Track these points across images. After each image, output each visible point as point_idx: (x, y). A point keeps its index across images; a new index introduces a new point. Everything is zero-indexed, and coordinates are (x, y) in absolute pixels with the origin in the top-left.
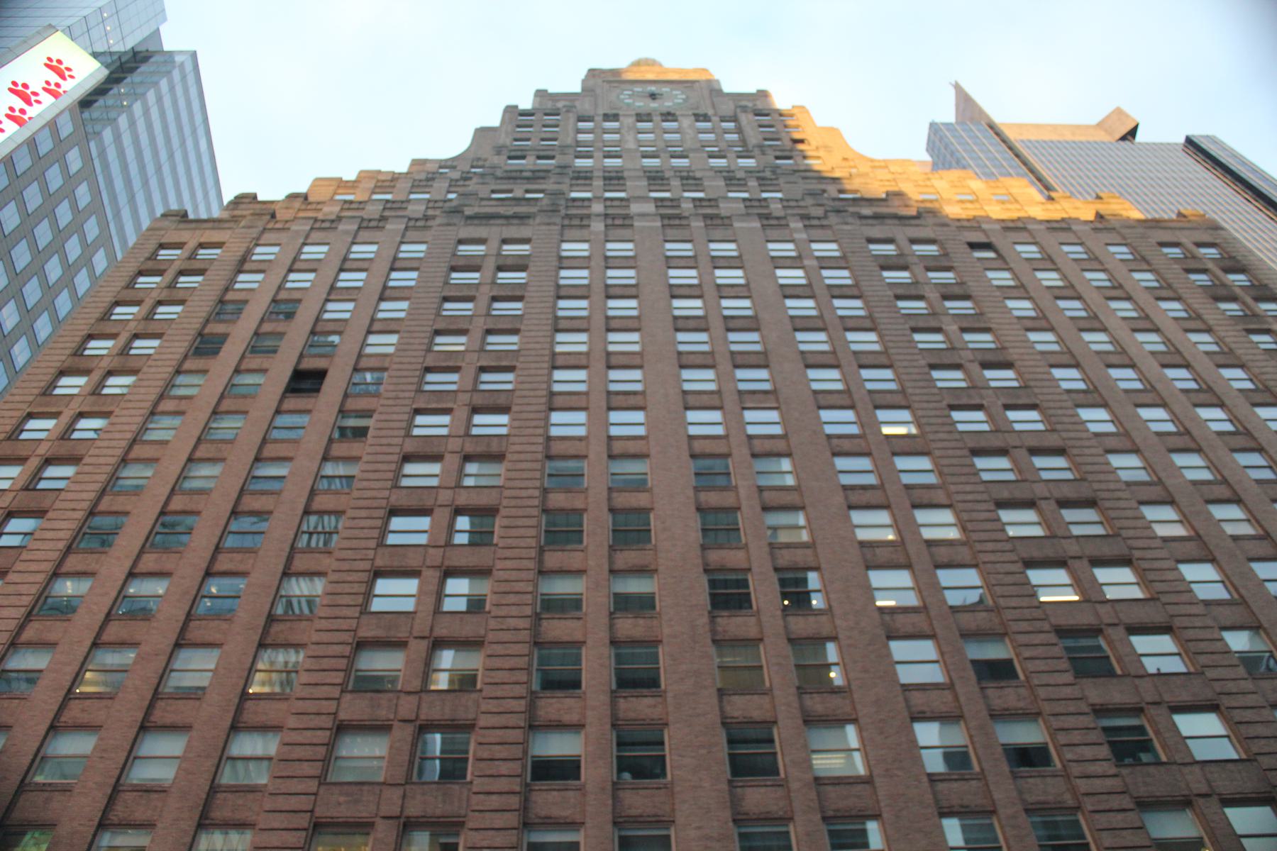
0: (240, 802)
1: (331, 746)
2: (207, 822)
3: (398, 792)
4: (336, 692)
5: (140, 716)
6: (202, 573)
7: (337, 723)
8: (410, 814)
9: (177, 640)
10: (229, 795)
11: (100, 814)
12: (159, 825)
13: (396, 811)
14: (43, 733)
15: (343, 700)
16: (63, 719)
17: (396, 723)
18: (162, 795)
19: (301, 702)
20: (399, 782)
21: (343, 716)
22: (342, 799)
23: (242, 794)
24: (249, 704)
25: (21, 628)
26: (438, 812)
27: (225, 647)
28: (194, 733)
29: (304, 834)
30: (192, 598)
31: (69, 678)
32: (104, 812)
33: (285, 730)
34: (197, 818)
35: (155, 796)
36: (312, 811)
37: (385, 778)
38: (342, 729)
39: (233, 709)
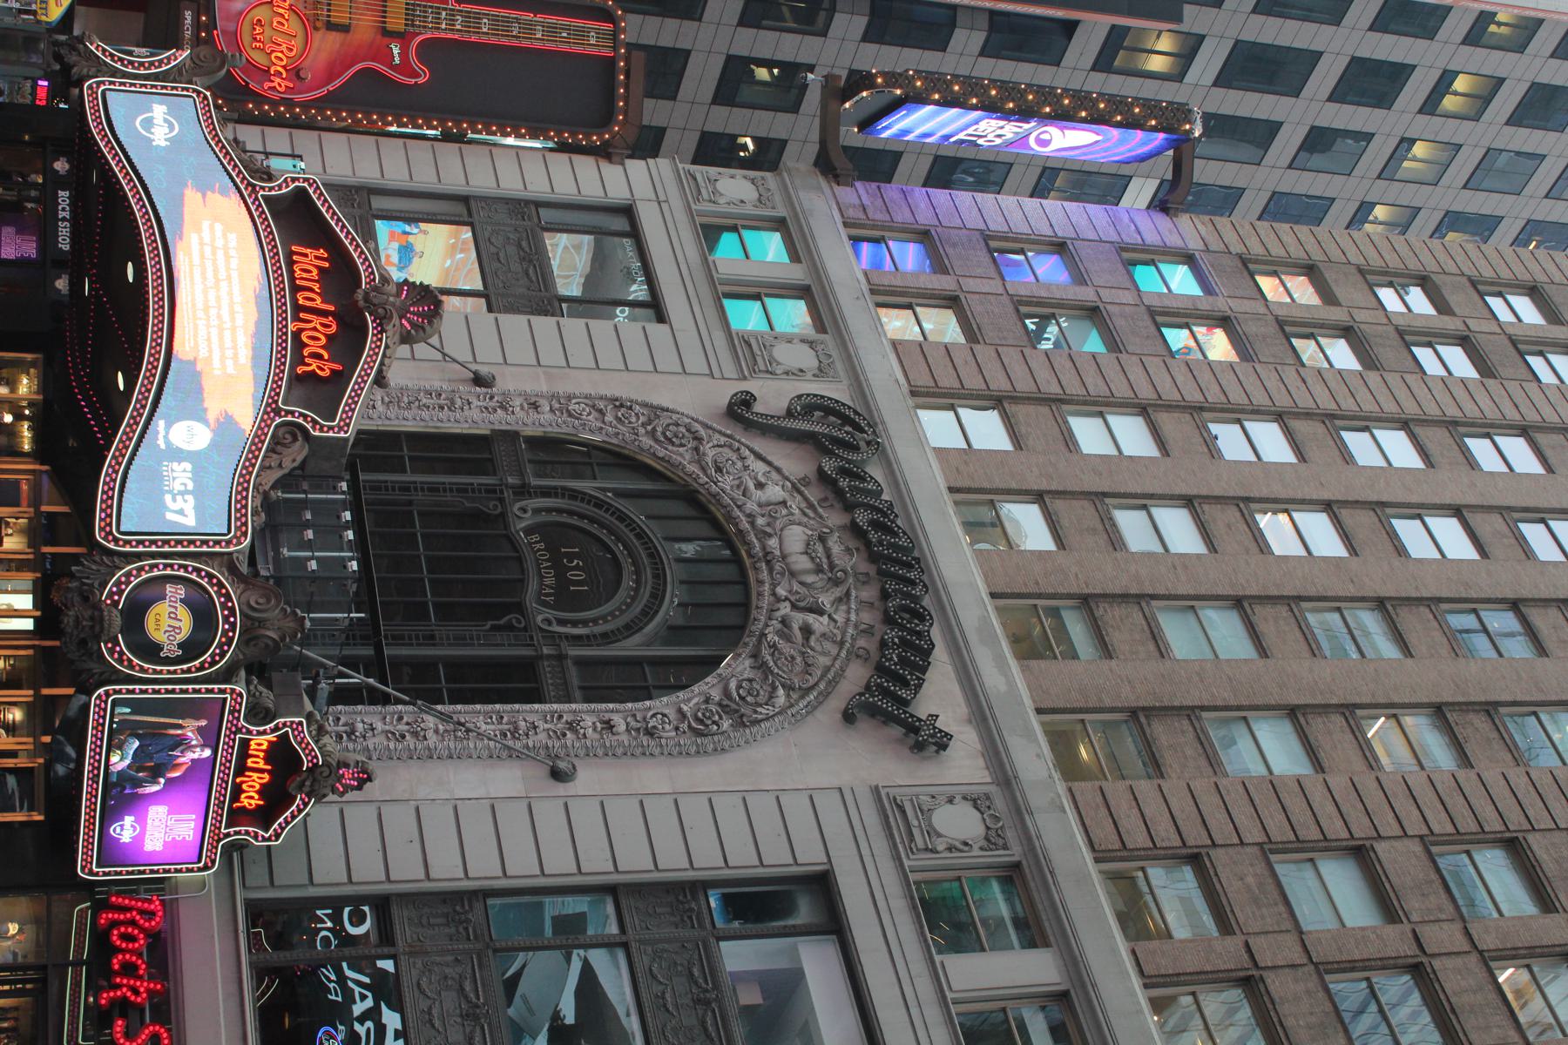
0: (1189, 752)
1: (1327, 846)
2: (1143, 719)
3: (1297, 956)
4: (1415, 826)
5: (1253, 590)
6: (1510, 595)
7: (1368, 843)
8: (1268, 981)
9: (1390, 598)
10: (1191, 735)
11: (1098, 591)
12: (1113, 663)
13: (1264, 959)
14: (1177, 491)
15: (1406, 841)
16: (1206, 507)
17: (1407, 927)
18: (1157, 654)
19: (1376, 784)
20: (1314, 955)
21: (1381, 847)
22: (1250, 880)
23: (1201, 751)
24: (1338, 720)
25: (1308, 415)
26: (1289, 1022)
27: (1409, 661)
28: (1261, 662)
29: (1177, 842)
30: (1464, 595)
31: (1265, 493)
32: (1104, 596)
33: (1320, 777)
34: (1141, 704)
35: (1152, 647)
36: (1214, 845)
37: (1310, 932)
38: (1361, 854)
39: (1319, 700)
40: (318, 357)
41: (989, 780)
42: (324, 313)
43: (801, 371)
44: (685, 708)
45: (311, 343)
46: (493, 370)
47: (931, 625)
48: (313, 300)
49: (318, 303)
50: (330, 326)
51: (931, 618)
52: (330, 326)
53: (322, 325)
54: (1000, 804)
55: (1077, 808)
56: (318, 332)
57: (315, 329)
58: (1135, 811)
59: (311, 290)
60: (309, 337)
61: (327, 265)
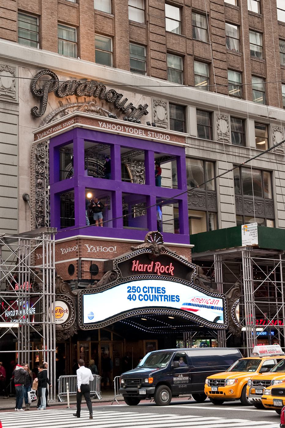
22: (174, 41)
40: (168, 269)
41: (150, 98)
42: (154, 265)
43: (13, 81)
44: (138, 174)
45: (164, 270)
46: (22, 194)
47: (115, 91)
48: (150, 267)
49: (151, 266)
50: (158, 264)
51: (113, 90)
52: (158, 264)
53: (158, 266)
54: (156, 98)
55: (156, 77)
56: (159, 267)
57: (159, 268)
58: (158, 61)
59: (147, 267)
60: (162, 270)
61: (138, 261)
